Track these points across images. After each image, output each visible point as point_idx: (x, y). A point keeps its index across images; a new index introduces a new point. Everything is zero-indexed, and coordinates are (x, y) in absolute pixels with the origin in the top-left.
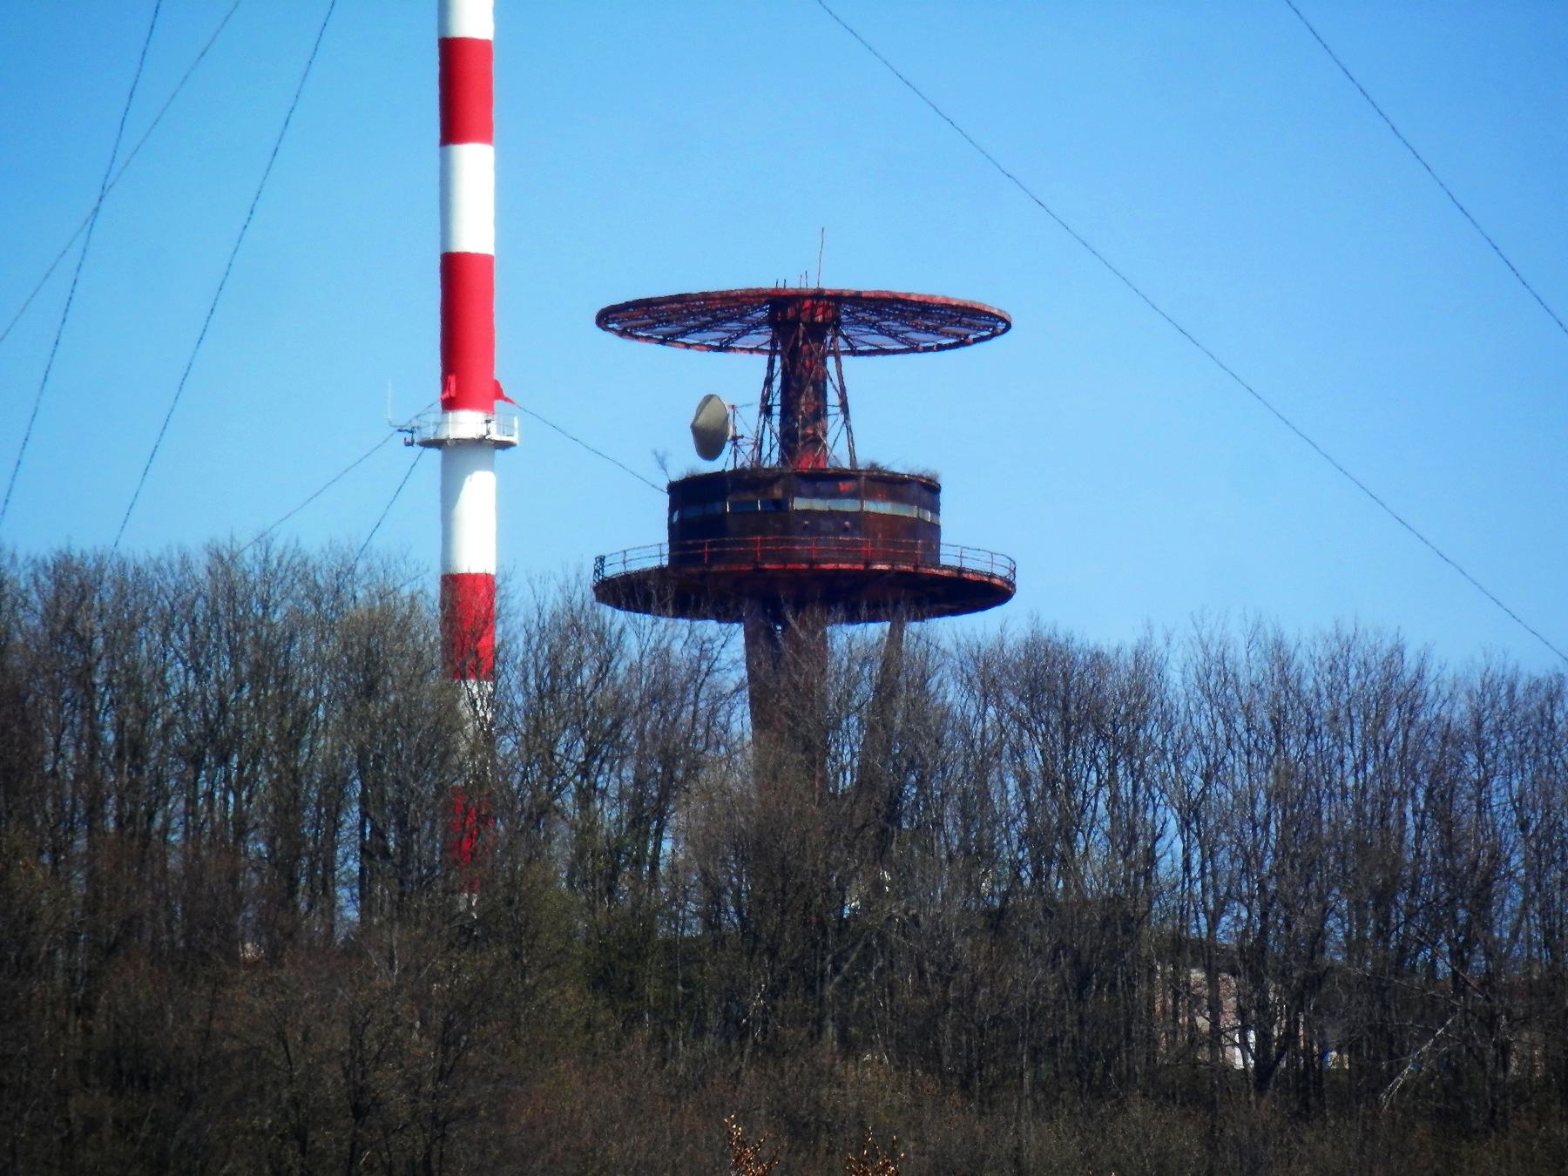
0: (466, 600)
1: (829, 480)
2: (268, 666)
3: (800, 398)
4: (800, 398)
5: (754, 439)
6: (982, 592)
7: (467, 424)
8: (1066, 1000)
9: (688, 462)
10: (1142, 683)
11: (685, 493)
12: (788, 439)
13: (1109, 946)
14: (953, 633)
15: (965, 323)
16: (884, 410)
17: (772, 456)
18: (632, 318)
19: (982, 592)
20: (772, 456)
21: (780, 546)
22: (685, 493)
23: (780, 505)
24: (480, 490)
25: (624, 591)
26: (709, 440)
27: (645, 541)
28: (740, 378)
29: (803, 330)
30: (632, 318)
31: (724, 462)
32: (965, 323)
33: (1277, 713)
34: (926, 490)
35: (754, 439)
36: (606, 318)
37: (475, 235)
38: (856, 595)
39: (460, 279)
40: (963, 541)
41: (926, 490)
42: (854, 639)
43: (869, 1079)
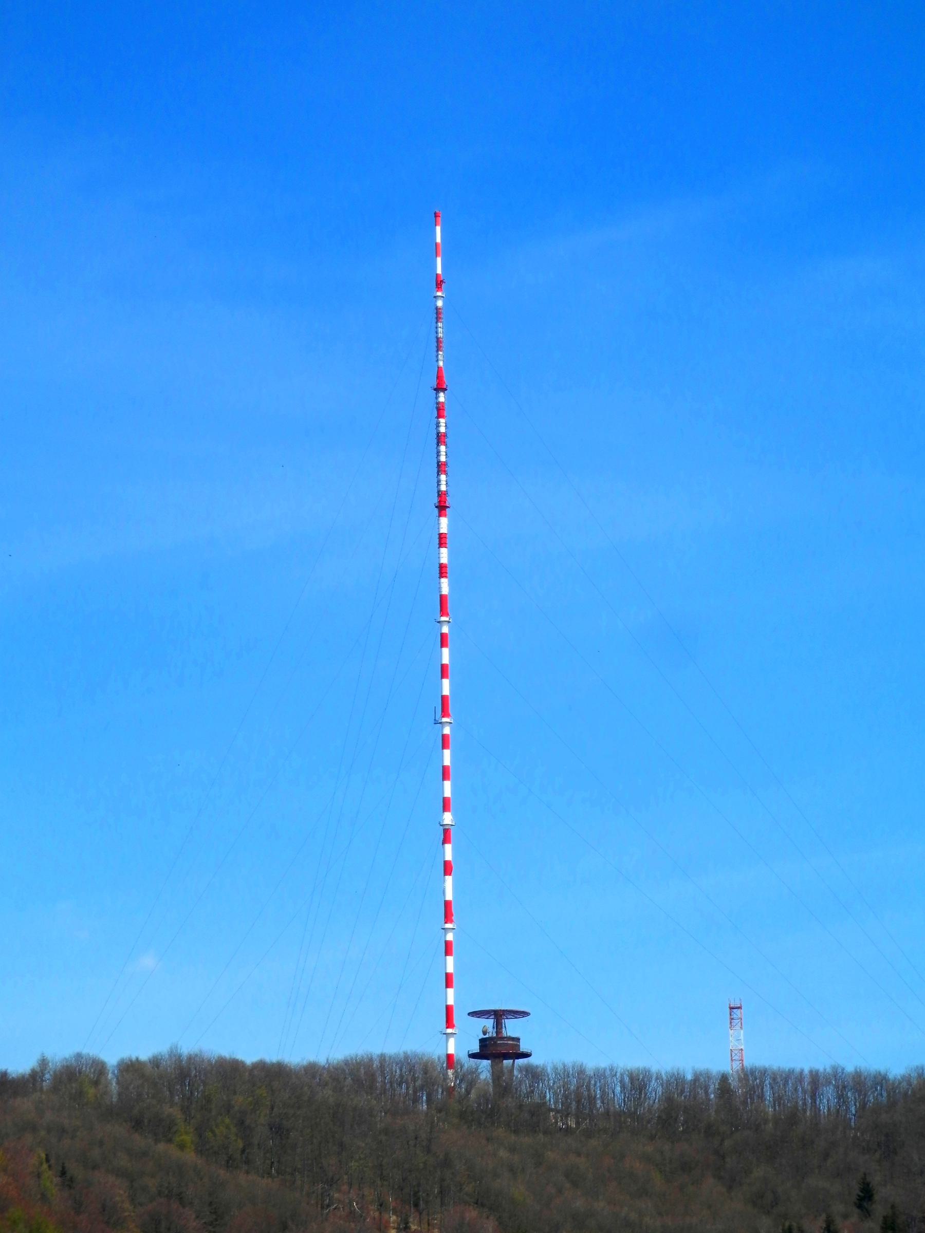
0: (450, 1057)
1: (503, 1038)
2: (412, 1069)
3: (498, 1026)
4: (498, 1026)
5: (492, 1033)
6: (526, 1055)
7: (449, 1031)
8: (533, 1118)
9: (482, 1036)
10: (544, 1069)
11: (482, 1041)
12: (497, 1032)
13: (539, 1110)
14: (520, 1062)
15: (524, 1014)
16: (512, 1028)
17: (495, 1035)
18: (474, 1014)
19: (526, 1055)
20: (495, 1035)
21: (496, 1049)
22: (482, 1041)
23: (495, 1043)
24: (452, 1041)
25: (473, 1056)
26: (485, 1033)
27: (476, 1048)
28: (489, 1023)
29: (499, 1016)
30: (474, 1014)
31: (487, 1036)
32: (524, 1014)
33: (564, 1074)
34: (518, 1040)
35: (492, 1033)
36: (469, 1014)
37: (450, 1002)
38: (506, 1056)
39: (449, 1010)
40: (524, 1048)
41: (518, 1040)
42: (507, 1063)
43: (500, 1132)
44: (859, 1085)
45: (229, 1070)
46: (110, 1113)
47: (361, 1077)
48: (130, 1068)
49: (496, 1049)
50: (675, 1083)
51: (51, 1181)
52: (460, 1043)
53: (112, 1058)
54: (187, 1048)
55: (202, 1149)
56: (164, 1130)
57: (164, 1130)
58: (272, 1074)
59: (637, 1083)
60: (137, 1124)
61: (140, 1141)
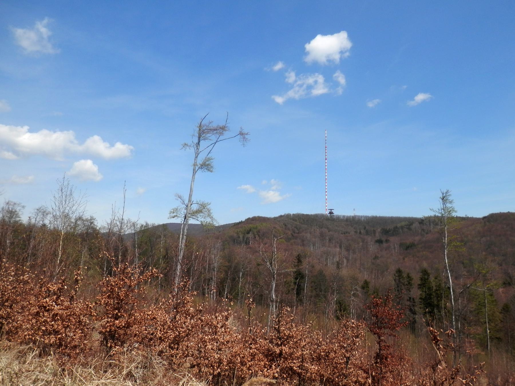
16: (332, 211)
21: (331, 213)
29: (331, 210)
33: (336, 216)
44: (366, 217)
45: (303, 215)
46: (291, 219)
47: (316, 216)
48: (293, 214)
49: (331, 213)
50: (348, 217)
51: (284, 226)
52: (327, 212)
53: (292, 213)
54: (299, 213)
55: (300, 222)
56: (296, 221)
57: (296, 221)
58: (307, 215)
59: (344, 216)
60: (293, 220)
61: (293, 222)
